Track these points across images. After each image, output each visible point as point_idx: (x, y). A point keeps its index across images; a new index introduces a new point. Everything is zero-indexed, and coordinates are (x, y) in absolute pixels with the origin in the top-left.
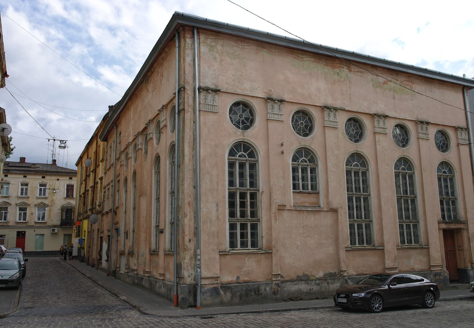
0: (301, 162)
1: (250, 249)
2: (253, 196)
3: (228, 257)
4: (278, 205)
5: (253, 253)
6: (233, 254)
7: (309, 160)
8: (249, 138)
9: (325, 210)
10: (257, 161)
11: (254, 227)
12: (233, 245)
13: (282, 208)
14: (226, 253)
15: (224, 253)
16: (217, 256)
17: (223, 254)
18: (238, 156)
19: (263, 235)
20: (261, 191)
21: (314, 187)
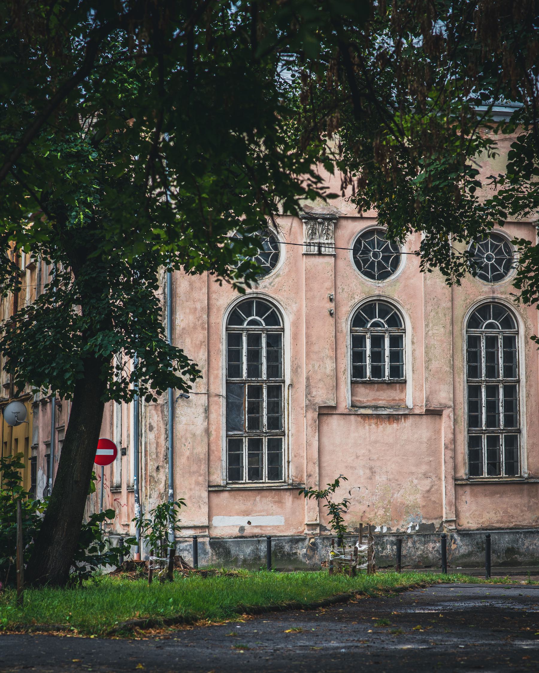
0: (371, 326)
1: (265, 481)
2: (275, 391)
3: (226, 495)
4: (320, 408)
5: (270, 489)
6: (232, 490)
7: (388, 322)
8: (265, 291)
9: (417, 411)
10: (283, 330)
11: (276, 445)
12: (234, 474)
13: (325, 412)
14: (222, 489)
15: (216, 489)
16: (206, 494)
17: (214, 490)
18: (246, 323)
19: (290, 460)
20: (288, 382)
21: (397, 371)
